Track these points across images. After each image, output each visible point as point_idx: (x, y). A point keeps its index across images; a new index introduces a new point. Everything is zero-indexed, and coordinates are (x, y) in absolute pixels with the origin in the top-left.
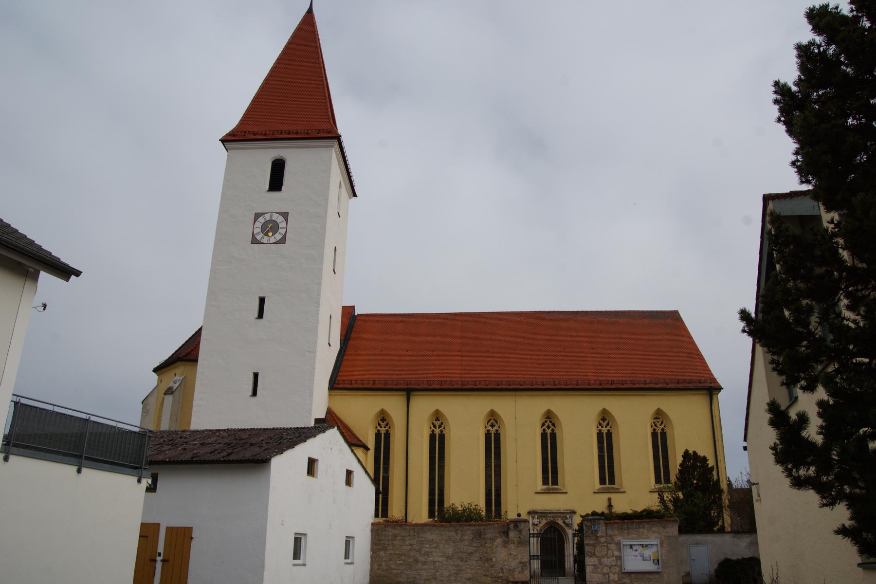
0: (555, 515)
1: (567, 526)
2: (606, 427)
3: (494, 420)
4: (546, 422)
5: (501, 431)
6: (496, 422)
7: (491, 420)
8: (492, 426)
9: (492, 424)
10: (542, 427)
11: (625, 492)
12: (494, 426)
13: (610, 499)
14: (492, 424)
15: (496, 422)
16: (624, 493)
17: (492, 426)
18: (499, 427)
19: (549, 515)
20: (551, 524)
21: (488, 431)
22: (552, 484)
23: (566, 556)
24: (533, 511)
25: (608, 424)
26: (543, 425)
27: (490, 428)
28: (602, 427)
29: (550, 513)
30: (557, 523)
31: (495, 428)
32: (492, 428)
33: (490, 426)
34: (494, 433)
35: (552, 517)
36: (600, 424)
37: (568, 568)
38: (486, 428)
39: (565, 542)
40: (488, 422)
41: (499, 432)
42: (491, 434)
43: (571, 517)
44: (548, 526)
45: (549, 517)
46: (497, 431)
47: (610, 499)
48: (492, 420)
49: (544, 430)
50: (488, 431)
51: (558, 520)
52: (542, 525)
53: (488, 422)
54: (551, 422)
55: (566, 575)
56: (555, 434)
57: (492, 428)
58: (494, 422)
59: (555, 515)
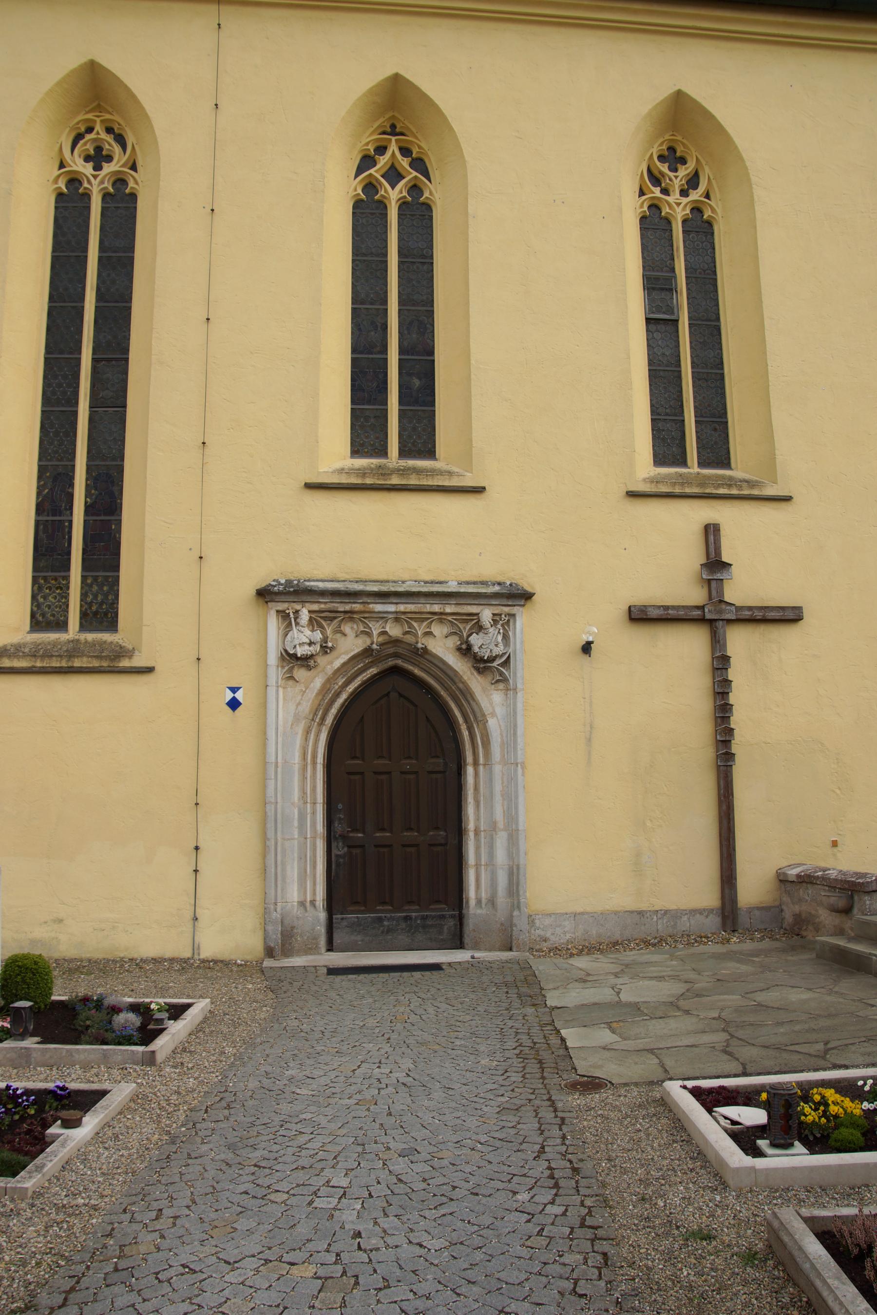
0: (411, 607)
1: (480, 671)
2: (684, 193)
3: (109, 130)
4: (381, 150)
5: (140, 183)
6: (121, 140)
7: (90, 130)
8: (98, 158)
9: (99, 149)
10: (359, 171)
11: (787, 499)
12: (109, 159)
13: (711, 532)
14: (99, 149)
15: (121, 140)
16: (783, 505)
17: (98, 158)
18: (134, 167)
19: (379, 608)
20: (391, 662)
21: (74, 181)
22: (404, 453)
23: (471, 835)
24: (289, 582)
25: (693, 181)
26: (366, 162)
27: (87, 169)
28: (665, 192)
29: (383, 596)
30: (425, 650)
31: (108, 168)
32: (98, 168)
33: (87, 159)
34: (106, 196)
35: (398, 618)
36: (655, 179)
37: (479, 902)
38: (62, 166)
39: (469, 759)
40: (78, 138)
41: (131, 184)
42: (87, 196)
43: (504, 622)
44: (373, 671)
45: (382, 617)
46: (120, 181)
47: (711, 532)
48: (98, 128)
49: (370, 187)
50: (74, 181)
51: (429, 634)
52: (337, 664)
53: (78, 138)
54: (405, 151)
55: (467, 940)
56: (427, 207)
57: (98, 168)
58: (109, 138)
59: (411, 607)
